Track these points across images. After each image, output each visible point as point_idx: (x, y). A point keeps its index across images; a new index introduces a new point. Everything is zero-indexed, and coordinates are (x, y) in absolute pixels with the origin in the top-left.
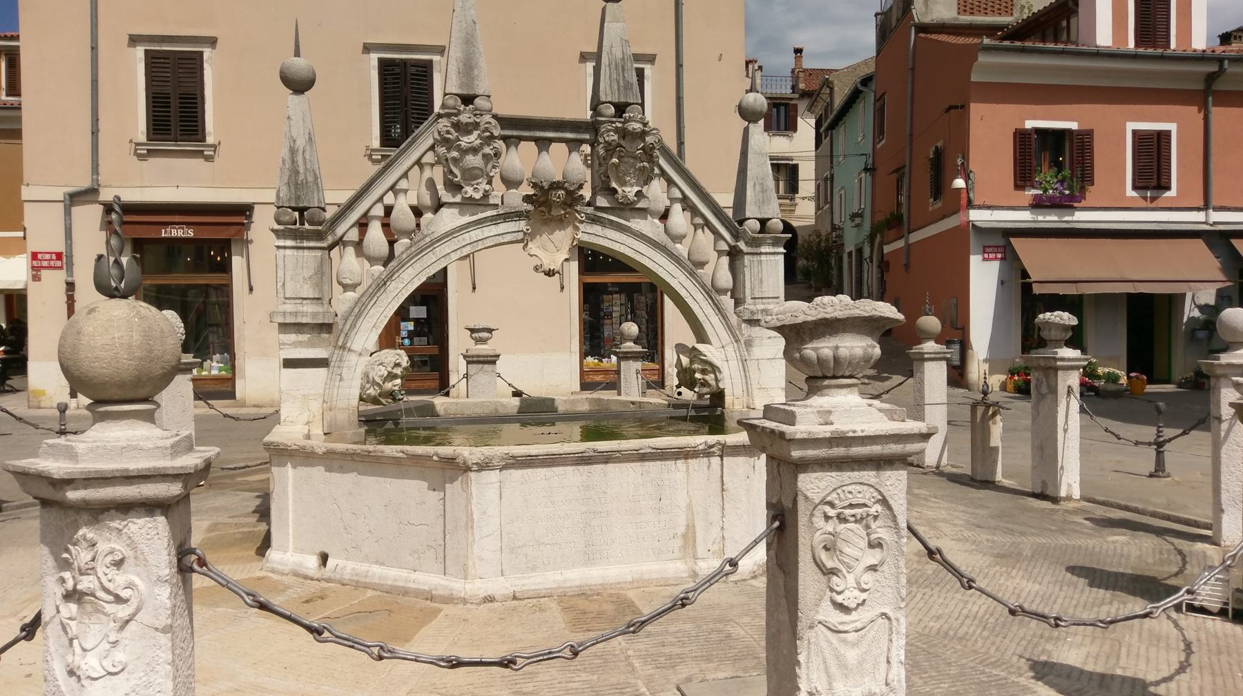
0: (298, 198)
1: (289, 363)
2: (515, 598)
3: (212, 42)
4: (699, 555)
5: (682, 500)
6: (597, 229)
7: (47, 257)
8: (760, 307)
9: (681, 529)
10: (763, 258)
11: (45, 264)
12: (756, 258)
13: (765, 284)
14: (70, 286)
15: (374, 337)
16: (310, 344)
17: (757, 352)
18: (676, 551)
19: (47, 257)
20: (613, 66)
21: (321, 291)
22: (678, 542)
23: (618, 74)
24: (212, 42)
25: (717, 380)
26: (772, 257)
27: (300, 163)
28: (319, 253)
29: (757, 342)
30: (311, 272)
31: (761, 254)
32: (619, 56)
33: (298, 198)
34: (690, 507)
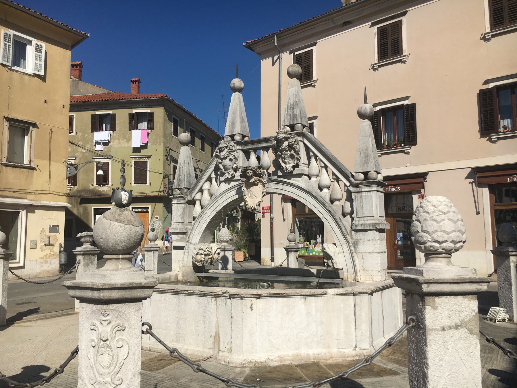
0: (179, 185)
1: (176, 248)
2: (150, 350)
3: (315, 118)
4: (221, 349)
5: (214, 320)
6: (280, 186)
7: (266, 208)
8: (361, 222)
9: (213, 334)
10: (364, 194)
11: (266, 211)
12: (359, 194)
13: (365, 209)
14: (272, 219)
15: (199, 237)
16: (180, 240)
17: (361, 248)
18: (211, 344)
19: (266, 208)
20: (289, 108)
21: (184, 220)
22: (212, 340)
23: (291, 112)
24: (315, 118)
25: (333, 263)
26: (369, 194)
27: (181, 172)
28: (183, 205)
29: (361, 243)
30: (181, 213)
31: (362, 192)
32: (292, 103)
33: (179, 185)
34: (217, 322)
